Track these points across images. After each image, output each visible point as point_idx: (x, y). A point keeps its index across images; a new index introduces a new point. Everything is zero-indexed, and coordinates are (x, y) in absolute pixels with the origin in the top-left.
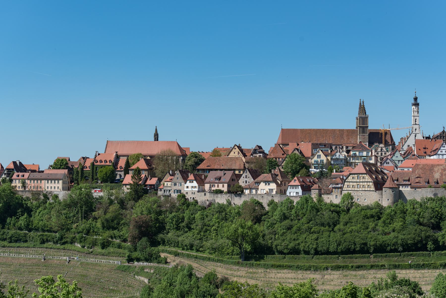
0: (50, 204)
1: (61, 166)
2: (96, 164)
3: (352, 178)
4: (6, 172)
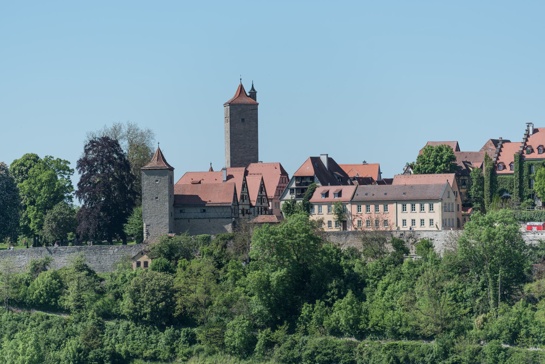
0: (412, 265)
1: (436, 164)
2: (527, 156)
4: (294, 186)
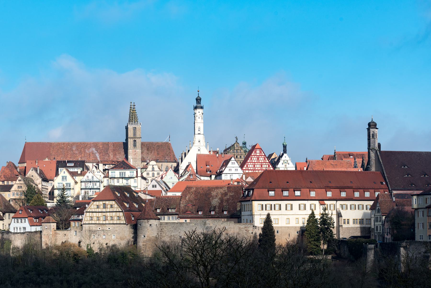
3: (95, 207)
